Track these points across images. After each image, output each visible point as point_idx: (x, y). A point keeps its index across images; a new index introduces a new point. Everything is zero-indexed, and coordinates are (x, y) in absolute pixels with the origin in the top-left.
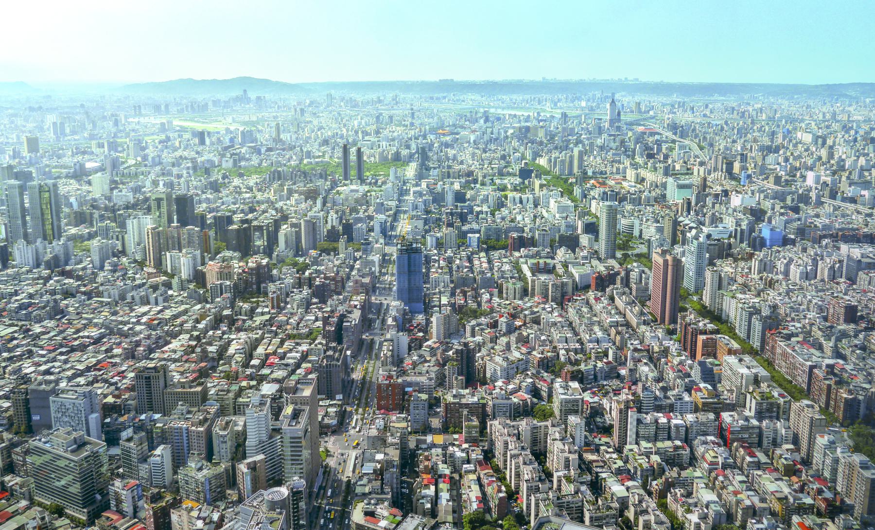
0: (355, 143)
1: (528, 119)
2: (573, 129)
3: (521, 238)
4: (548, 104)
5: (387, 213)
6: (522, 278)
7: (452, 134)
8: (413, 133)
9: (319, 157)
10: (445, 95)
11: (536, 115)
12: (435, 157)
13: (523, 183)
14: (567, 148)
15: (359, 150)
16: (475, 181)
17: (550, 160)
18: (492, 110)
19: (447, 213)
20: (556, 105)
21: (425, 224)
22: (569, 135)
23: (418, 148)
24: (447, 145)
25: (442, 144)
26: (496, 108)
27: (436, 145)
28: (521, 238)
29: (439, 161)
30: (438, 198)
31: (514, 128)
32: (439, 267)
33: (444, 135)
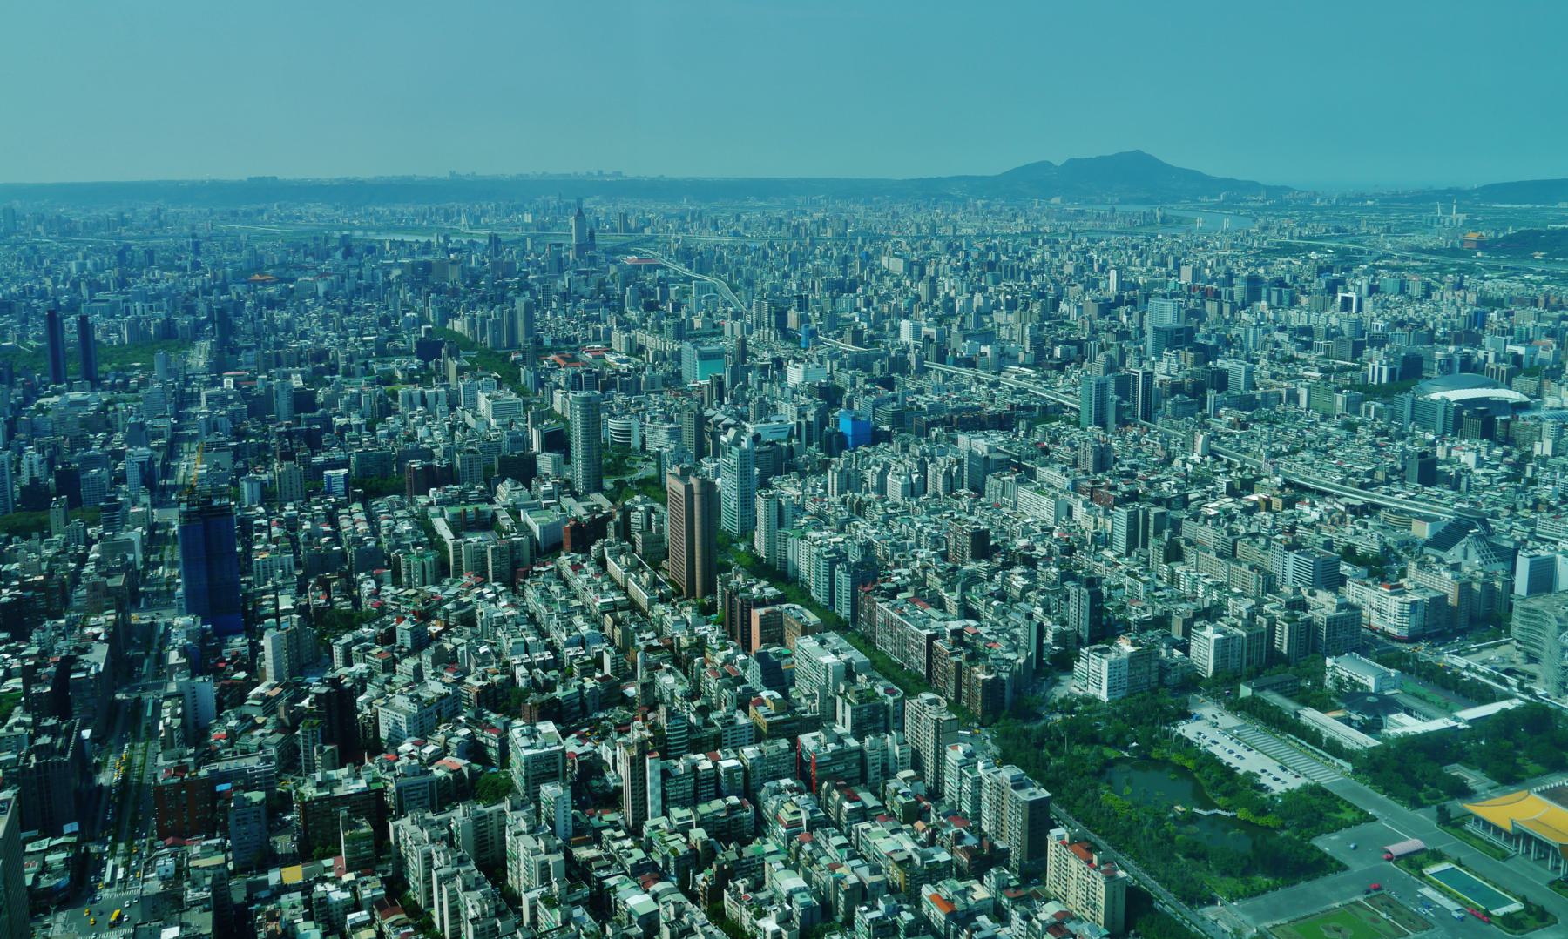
0: (73, 307)
2: (511, 264)
3: (428, 469)
4: (463, 221)
6: (436, 543)
7: (281, 280)
8: (199, 282)
10: (261, 207)
12: (248, 328)
13: (426, 367)
14: (502, 298)
15: (84, 319)
17: (472, 324)
18: (358, 234)
19: (280, 434)
20: (477, 220)
21: (236, 458)
22: (504, 276)
24: (272, 303)
27: (248, 304)
29: (257, 335)
30: (260, 406)
32: (270, 540)
33: (264, 283)
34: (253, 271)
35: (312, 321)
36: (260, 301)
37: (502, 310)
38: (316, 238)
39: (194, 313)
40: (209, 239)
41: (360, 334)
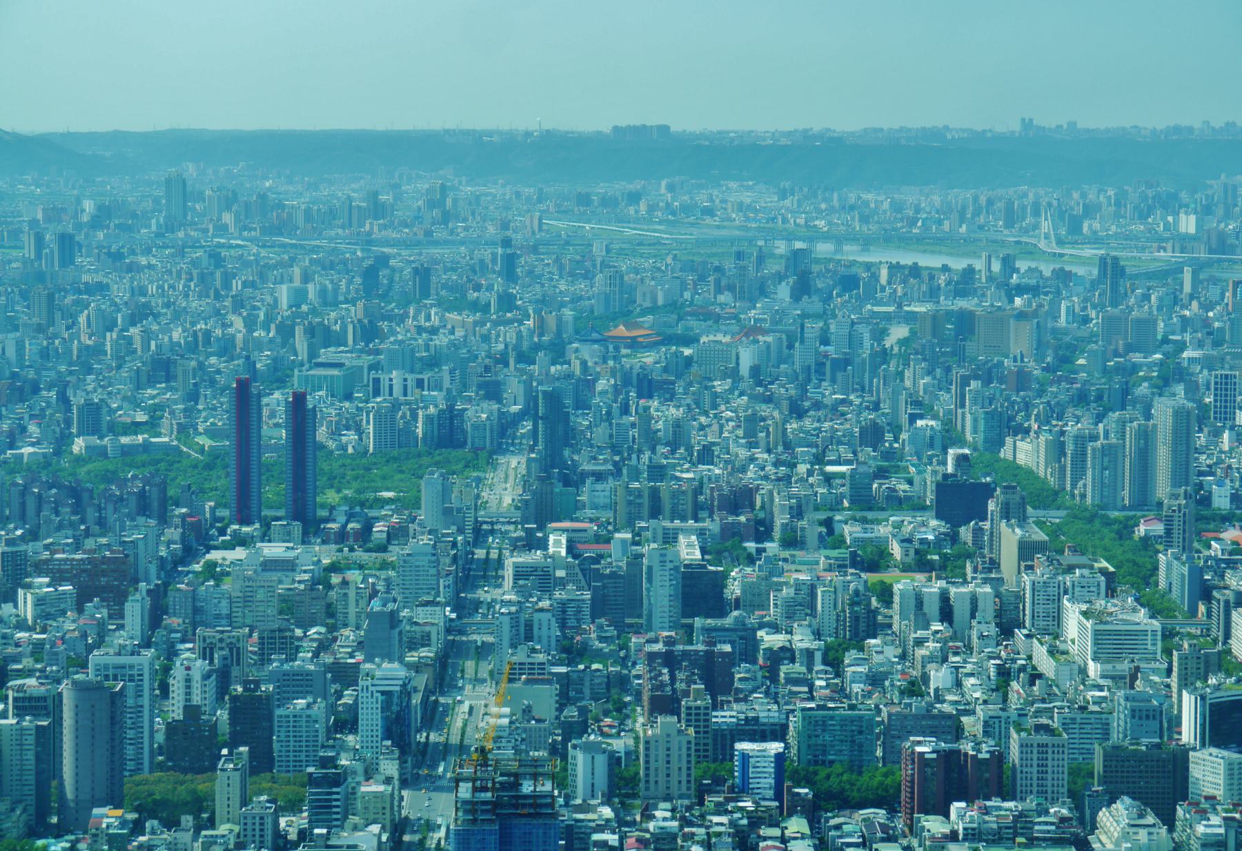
1: (965, 283)
2: (1147, 324)
3: (950, 760)
4: (1046, 226)
5: (412, 657)
7: (668, 340)
8: (511, 337)
9: (135, 427)
10: (637, 185)
11: (996, 267)
12: (600, 434)
13: (954, 538)
14: (1124, 398)
15: (298, 402)
16: (762, 530)
17: (1057, 449)
18: (824, 249)
19: (652, 656)
20: (1075, 226)
21: (564, 700)
22: (1130, 348)
23: (531, 399)
24: (647, 386)
25: (627, 381)
26: (839, 240)
27: (602, 384)
28: (950, 760)
29: (615, 449)
31: (911, 318)
33: (634, 344)
34: (614, 318)
35: (724, 427)
37: (1122, 423)
38: (739, 256)
39: (499, 401)
40: (534, 249)
41: (819, 459)
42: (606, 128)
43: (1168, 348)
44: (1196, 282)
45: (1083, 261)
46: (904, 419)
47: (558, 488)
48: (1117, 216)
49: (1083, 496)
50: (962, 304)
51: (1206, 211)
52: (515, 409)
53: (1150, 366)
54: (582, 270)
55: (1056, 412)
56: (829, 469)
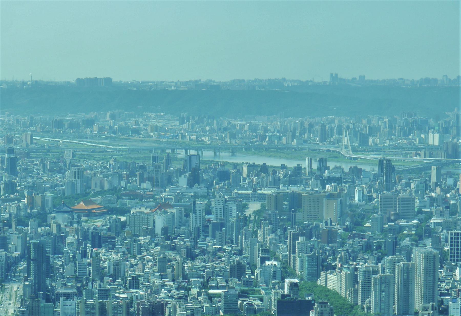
1: (295, 176)
2: (409, 201)
4: (345, 140)
7: (111, 211)
8: (14, 209)
10: (91, 115)
11: (315, 166)
12: (69, 270)
14: (394, 247)
17: (353, 279)
18: (208, 155)
20: (364, 140)
22: (398, 217)
23: (26, 248)
24: (98, 240)
25: (85, 237)
26: (217, 150)
27: (70, 239)
29: (78, 279)
31: (262, 197)
33: (89, 214)
34: (77, 198)
35: (145, 265)
36: (85, 236)
37: (393, 263)
38: (155, 159)
39: (6, 249)
40: (28, 155)
42: (73, 80)
43: (422, 216)
44: (439, 175)
45: (369, 162)
46: (258, 261)
47: (43, 303)
48: (390, 134)
49: (369, 308)
50: (294, 189)
51: (445, 131)
52: (16, 254)
53: (410, 228)
54: (57, 168)
55: (352, 256)
56: (211, 291)
